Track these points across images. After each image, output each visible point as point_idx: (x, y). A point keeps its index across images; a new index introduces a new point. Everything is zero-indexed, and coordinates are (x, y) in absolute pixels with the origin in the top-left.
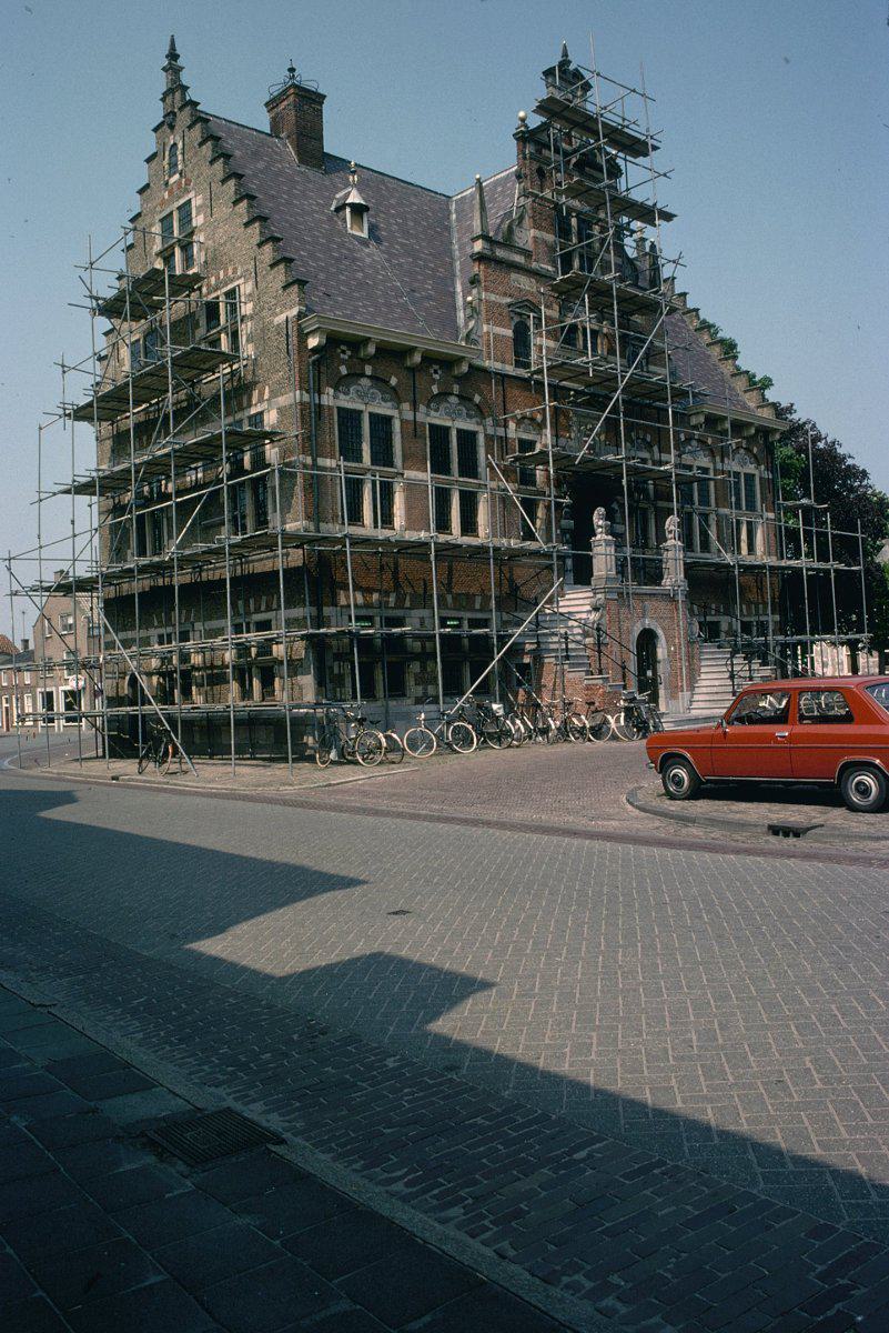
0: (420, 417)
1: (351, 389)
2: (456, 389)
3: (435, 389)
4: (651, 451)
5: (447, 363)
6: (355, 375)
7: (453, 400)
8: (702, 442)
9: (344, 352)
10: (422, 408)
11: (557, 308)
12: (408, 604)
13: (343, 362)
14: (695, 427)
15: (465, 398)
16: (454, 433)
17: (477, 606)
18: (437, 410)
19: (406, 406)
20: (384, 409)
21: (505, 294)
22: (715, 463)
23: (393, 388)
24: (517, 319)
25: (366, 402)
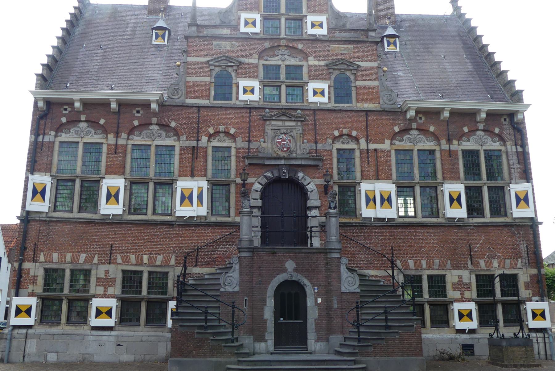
0: (121, 141)
1: (71, 131)
2: (155, 120)
3: (136, 123)
4: (358, 143)
5: (146, 105)
6: (73, 121)
7: (154, 128)
8: (422, 130)
9: (66, 109)
10: (124, 135)
11: (257, 57)
12: (96, 260)
13: (65, 115)
14: (411, 120)
15: (164, 126)
16: (153, 149)
17: (158, 263)
18: (140, 135)
19: (111, 136)
20: (96, 138)
21: (207, 56)
22: (439, 144)
23: (102, 126)
24: (217, 69)
25: (83, 135)
